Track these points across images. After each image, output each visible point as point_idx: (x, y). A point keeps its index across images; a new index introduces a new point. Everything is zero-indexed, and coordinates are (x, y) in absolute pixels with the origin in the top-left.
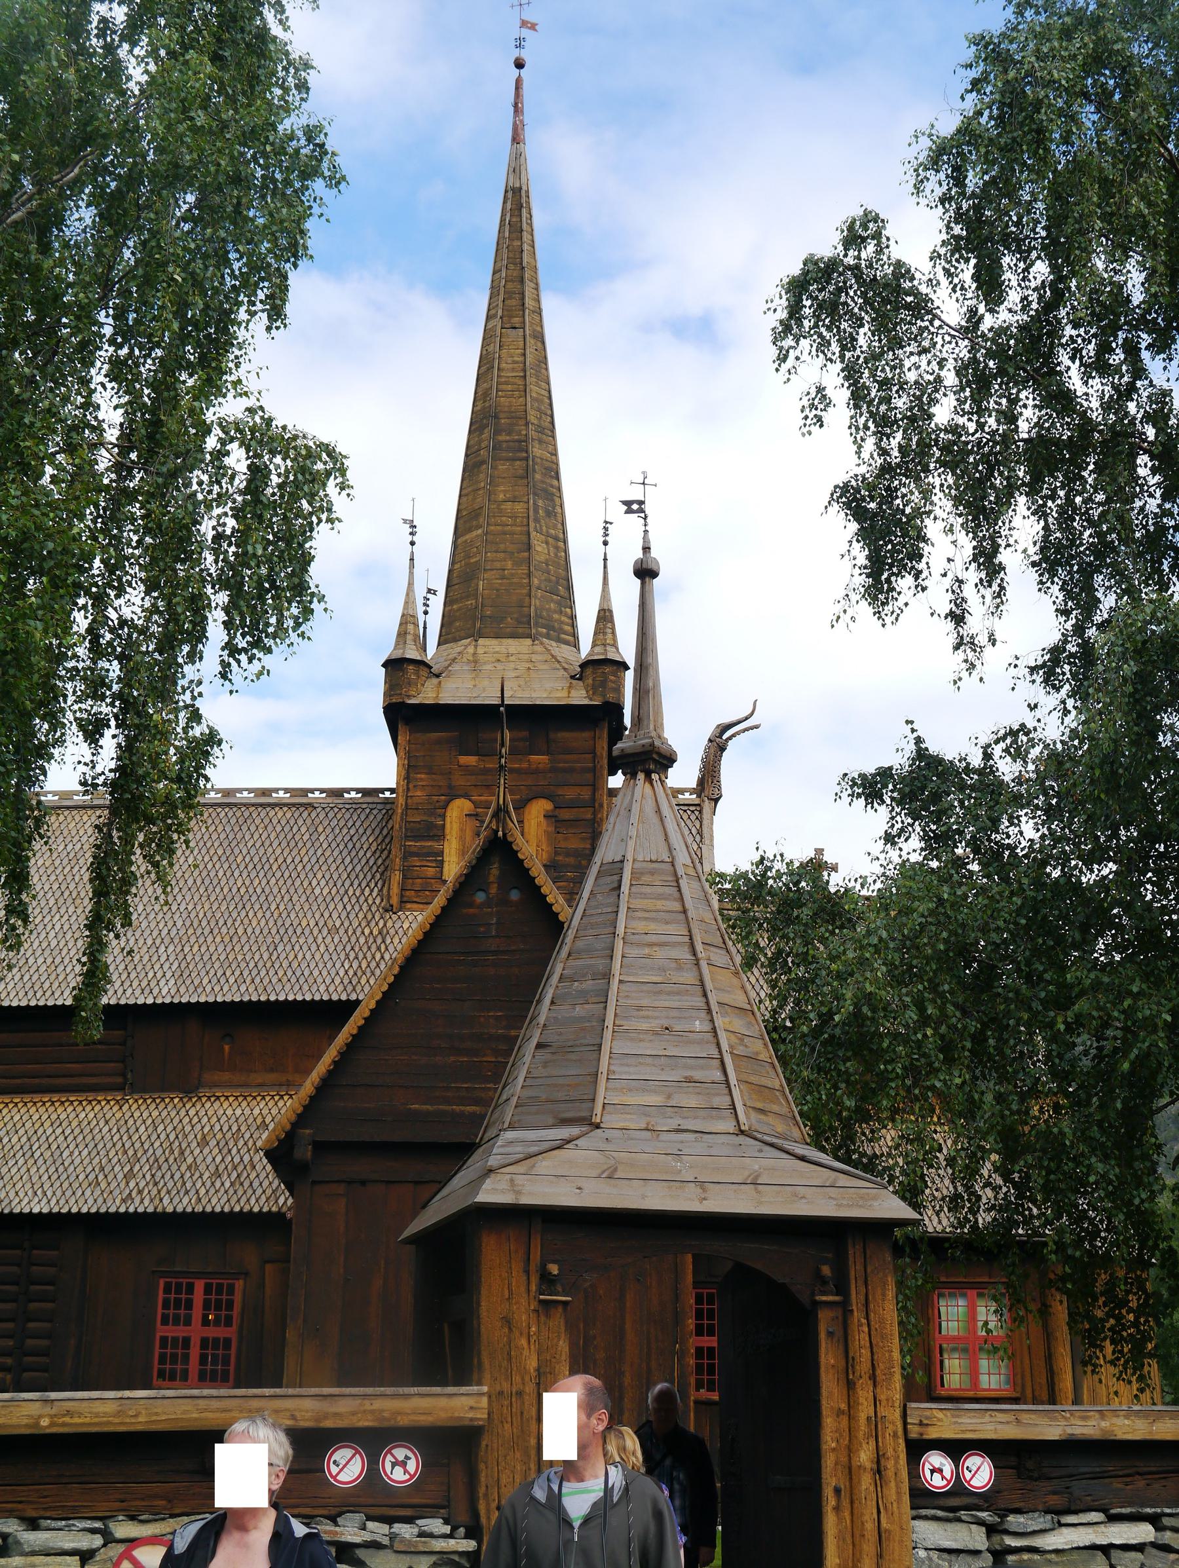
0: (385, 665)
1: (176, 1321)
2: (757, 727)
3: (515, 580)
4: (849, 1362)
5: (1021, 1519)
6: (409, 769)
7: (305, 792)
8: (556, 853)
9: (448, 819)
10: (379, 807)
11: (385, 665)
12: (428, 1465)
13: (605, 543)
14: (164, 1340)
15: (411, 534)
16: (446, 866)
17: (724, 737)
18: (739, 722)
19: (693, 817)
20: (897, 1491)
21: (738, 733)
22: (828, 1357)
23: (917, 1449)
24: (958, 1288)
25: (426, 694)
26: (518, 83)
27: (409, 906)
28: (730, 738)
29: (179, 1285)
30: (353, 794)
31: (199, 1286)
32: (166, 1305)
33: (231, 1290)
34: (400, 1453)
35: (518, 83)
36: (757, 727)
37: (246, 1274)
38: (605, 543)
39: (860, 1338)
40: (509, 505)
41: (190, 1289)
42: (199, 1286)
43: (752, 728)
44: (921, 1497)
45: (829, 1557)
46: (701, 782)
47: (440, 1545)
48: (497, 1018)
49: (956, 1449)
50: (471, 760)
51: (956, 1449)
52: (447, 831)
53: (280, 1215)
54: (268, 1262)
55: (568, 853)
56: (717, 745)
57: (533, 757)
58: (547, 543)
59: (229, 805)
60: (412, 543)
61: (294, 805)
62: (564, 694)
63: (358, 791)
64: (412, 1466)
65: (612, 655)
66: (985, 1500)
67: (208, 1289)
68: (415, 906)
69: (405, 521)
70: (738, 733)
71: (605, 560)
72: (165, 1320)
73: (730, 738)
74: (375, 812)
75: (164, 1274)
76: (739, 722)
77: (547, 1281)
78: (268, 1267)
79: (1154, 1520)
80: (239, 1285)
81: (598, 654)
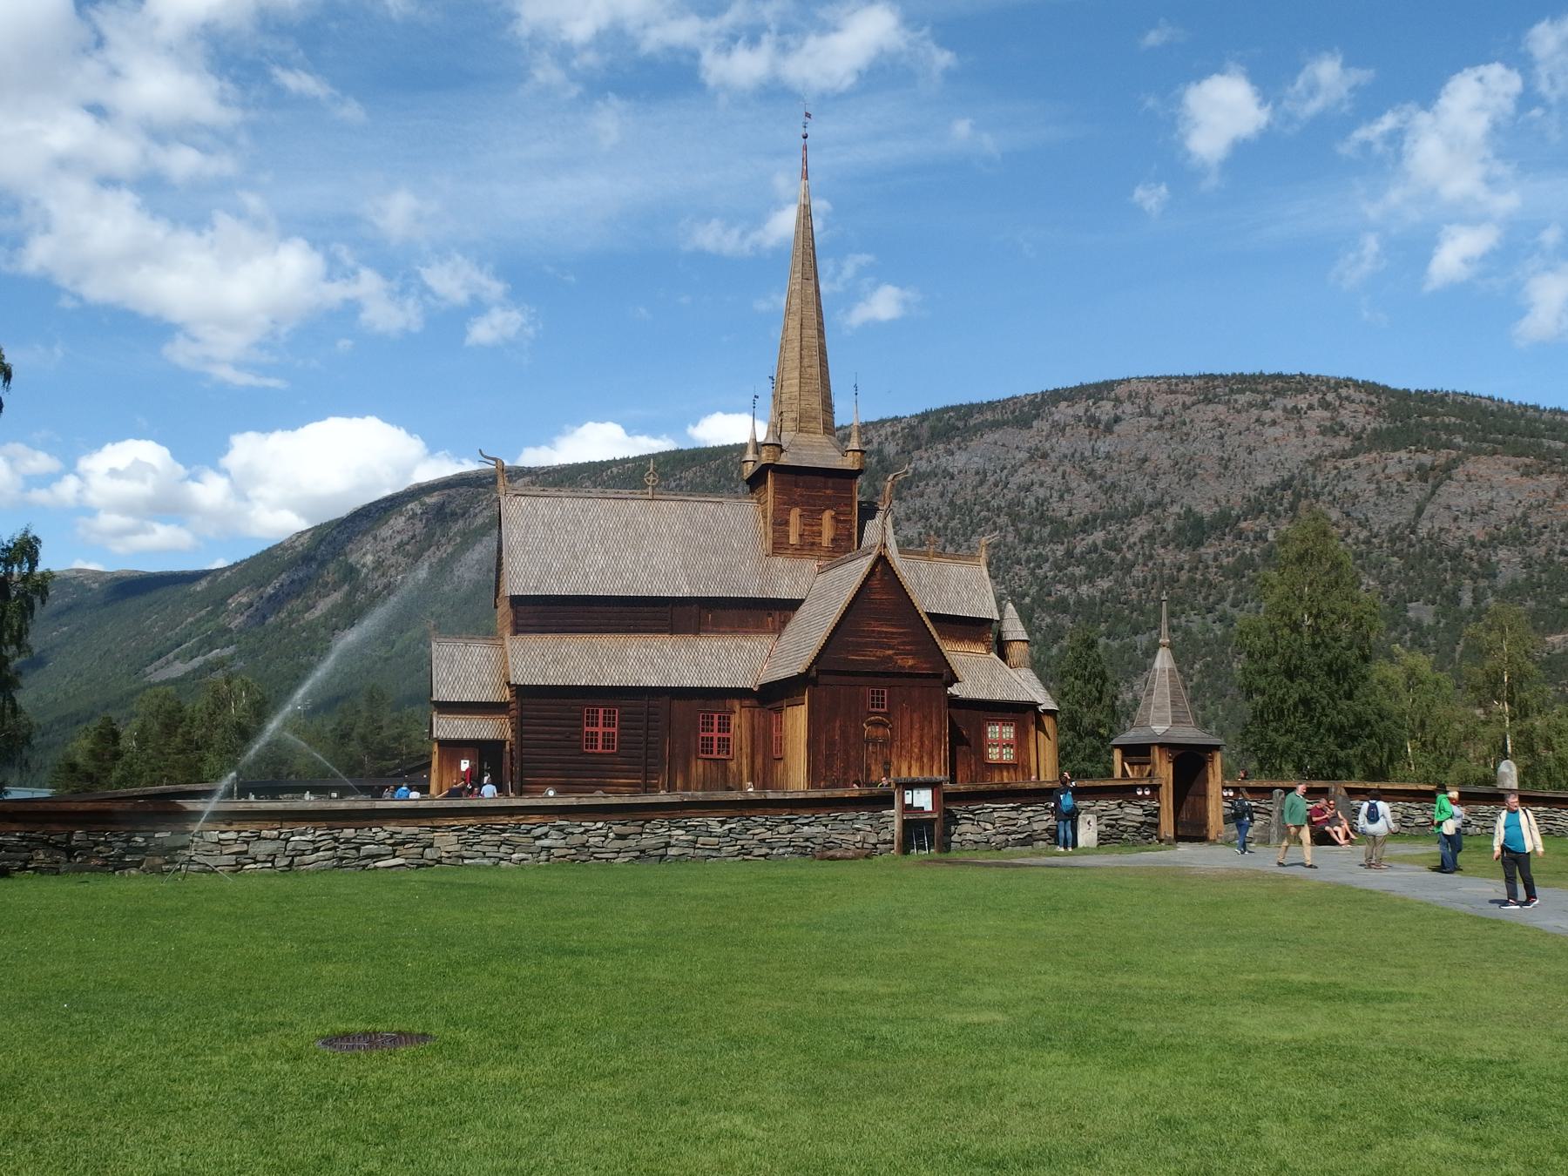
1: (708, 731)
8: (837, 535)
14: (703, 738)
16: (791, 538)
22: (1210, 770)
24: (995, 722)
25: (785, 460)
26: (805, 148)
31: (716, 716)
32: (703, 723)
35: (805, 148)
40: (808, 370)
42: (716, 716)
45: (1210, 808)
55: (841, 535)
57: (828, 492)
67: (719, 717)
72: (703, 731)
75: (702, 712)
78: (743, 710)
80: (732, 717)
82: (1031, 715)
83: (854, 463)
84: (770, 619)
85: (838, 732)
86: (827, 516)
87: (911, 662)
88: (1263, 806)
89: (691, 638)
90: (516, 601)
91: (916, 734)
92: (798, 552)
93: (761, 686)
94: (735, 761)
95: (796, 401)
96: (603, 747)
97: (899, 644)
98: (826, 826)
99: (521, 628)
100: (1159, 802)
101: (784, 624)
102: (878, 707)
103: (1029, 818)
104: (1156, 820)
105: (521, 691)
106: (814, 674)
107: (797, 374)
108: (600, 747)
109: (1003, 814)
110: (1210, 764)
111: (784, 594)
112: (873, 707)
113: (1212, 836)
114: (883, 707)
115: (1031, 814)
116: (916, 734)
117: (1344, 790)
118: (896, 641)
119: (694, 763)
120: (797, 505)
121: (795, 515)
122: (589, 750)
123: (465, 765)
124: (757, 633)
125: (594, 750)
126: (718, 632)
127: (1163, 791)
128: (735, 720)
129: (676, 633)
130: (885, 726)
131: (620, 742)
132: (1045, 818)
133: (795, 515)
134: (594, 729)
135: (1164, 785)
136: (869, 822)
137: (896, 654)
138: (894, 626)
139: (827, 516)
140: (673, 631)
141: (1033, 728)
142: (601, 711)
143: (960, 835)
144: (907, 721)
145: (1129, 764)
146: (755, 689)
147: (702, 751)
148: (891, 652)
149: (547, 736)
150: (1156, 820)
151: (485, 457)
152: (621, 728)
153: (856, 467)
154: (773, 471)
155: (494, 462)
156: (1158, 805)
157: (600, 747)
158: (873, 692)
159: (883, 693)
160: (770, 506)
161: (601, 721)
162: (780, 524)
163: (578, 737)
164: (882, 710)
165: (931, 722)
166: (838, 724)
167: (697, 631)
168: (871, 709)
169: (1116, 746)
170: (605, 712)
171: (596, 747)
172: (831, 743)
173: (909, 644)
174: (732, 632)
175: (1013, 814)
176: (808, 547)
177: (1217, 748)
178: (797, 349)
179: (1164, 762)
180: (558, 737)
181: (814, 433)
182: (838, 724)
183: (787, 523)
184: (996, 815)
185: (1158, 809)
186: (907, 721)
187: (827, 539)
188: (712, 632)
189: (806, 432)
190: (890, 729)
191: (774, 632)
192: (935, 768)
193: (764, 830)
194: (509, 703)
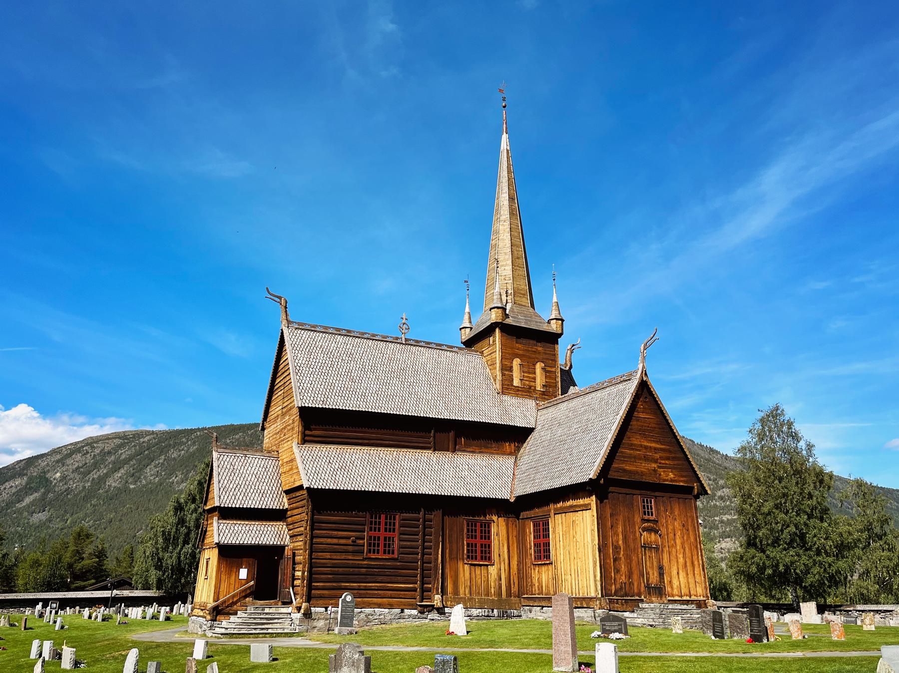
8: (546, 382)
25: (509, 321)
86: (539, 366)
87: (671, 476)
89: (449, 454)
90: (305, 412)
93: (519, 498)
97: (661, 458)
99: (307, 438)
101: (518, 449)
108: (381, 551)
111: (520, 423)
116: (678, 541)
118: (657, 456)
119: (461, 569)
121: (516, 362)
123: (243, 573)
128: (494, 530)
129: (439, 451)
133: (516, 362)
137: (659, 467)
138: (656, 442)
139: (539, 366)
142: (383, 516)
146: (512, 500)
147: (468, 557)
148: (654, 465)
149: (335, 541)
151: (271, 295)
153: (560, 332)
154: (500, 329)
157: (381, 551)
160: (498, 356)
161: (382, 527)
162: (506, 369)
163: (361, 542)
164: (652, 518)
167: (454, 451)
172: (616, 548)
173: (668, 459)
176: (527, 391)
180: (342, 541)
183: (511, 369)
187: (539, 385)
191: (510, 454)
194: (287, 510)
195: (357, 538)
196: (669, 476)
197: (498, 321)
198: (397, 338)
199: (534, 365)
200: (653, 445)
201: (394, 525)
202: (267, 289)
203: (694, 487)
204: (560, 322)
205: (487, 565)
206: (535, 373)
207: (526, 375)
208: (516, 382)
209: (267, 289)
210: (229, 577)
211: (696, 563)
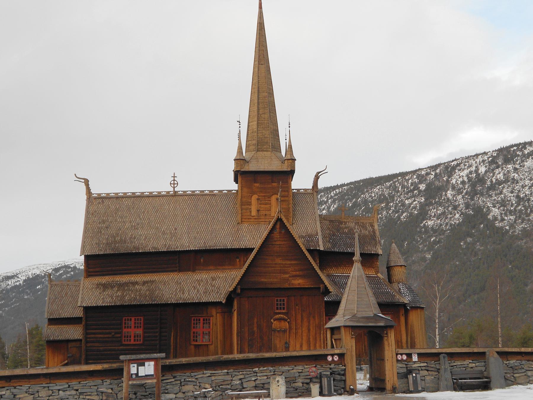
0: (234, 160)
2: (327, 172)
3: (265, 136)
4: (389, 344)
5: (410, 363)
6: (242, 187)
7: (213, 191)
9: (252, 200)
10: (232, 195)
11: (234, 160)
12: (339, 358)
13: (289, 127)
15: (240, 124)
17: (319, 175)
18: (323, 171)
19: (311, 197)
20: (395, 360)
21: (322, 174)
22: (386, 343)
23: (397, 354)
25: (246, 168)
27: (243, 222)
28: (320, 175)
29: (197, 319)
30: (225, 192)
33: (209, 320)
34: (336, 357)
36: (327, 172)
37: (213, 316)
38: (289, 127)
39: (390, 341)
40: (263, 116)
41: (199, 320)
43: (326, 173)
44: (398, 361)
45: (387, 368)
46: (313, 187)
47: (341, 368)
48: (280, 259)
49: (402, 354)
50: (257, 185)
51: (402, 354)
52: (252, 203)
53: (221, 302)
54: (218, 313)
56: (317, 177)
58: (273, 125)
59: (194, 195)
60: (240, 127)
61: (210, 195)
62: (280, 167)
63: (226, 190)
64: (337, 358)
65: (293, 158)
66: (405, 361)
68: (245, 222)
69: (238, 121)
70: (322, 174)
71: (289, 131)
73: (320, 175)
74: (231, 196)
76: (323, 171)
77: (352, 335)
78: (218, 314)
79: (426, 363)
81: (289, 157)
82: (402, 312)
83: (288, 167)
84: (238, 260)
85: (255, 325)
88: (432, 366)
91: (306, 324)
92: (256, 220)
94: (213, 345)
95: (256, 134)
96: (135, 341)
98: (77, 390)
100: (345, 366)
102: (281, 309)
103: (240, 379)
104: (343, 378)
105: (87, 309)
106: (239, 291)
107: (256, 119)
109: (220, 377)
110: (385, 338)
112: (277, 309)
113: (389, 386)
114: (284, 309)
115: (242, 377)
117: (496, 354)
120: (253, 193)
122: (126, 343)
124: (230, 269)
125: (129, 343)
126: (207, 270)
127: (347, 358)
130: (285, 320)
131: (144, 337)
132: (253, 379)
134: (129, 330)
135: (349, 353)
136: (111, 386)
140: (180, 271)
141: (403, 319)
143: (184, 393)
144: (299, 317)
145: (335, 339)
148: (287, 276)
149: (102, 336)
150: (343, 378)
152: (144, 329)
154: (241, 174)
155: (83, 181)
156: (344, 368)
158: (277, 301)
159: (284, 300)
164: (284, 311)
165: (314, 317)
166: (255, 320)
168: (277, 311)
169: (328, 328)
170: (135, 319)
171: (130, 340)
174: (214, 270)
175: (229, 378)
177: (391, 327)
178: (256, 104)
179: (349, 338)
180: (106, 336)
181: (267, 151)
182: (255, 320)
183: (250, 204)
184: (213, 378)
185: (345, 369)
186: (299, 317)
188: (203, 270)
189: (262, 151)
190: (288, 322)
192: (317, 345)
193: (27, 395)
195: (116, 333)
196: (298, 282)
197: (238, 170)
198: (168, 192)
199: (270, 197)
200: (289, 262)
201: (140, 324)
202: (75, 174)
203: (320, 288)
204: (291, 161)
205: (207, 345)
206: (270, 204)
207: (262, 206)
208: (254, 213)
209: (75, 174)
210: (54, 359)
211: (318, 339)
